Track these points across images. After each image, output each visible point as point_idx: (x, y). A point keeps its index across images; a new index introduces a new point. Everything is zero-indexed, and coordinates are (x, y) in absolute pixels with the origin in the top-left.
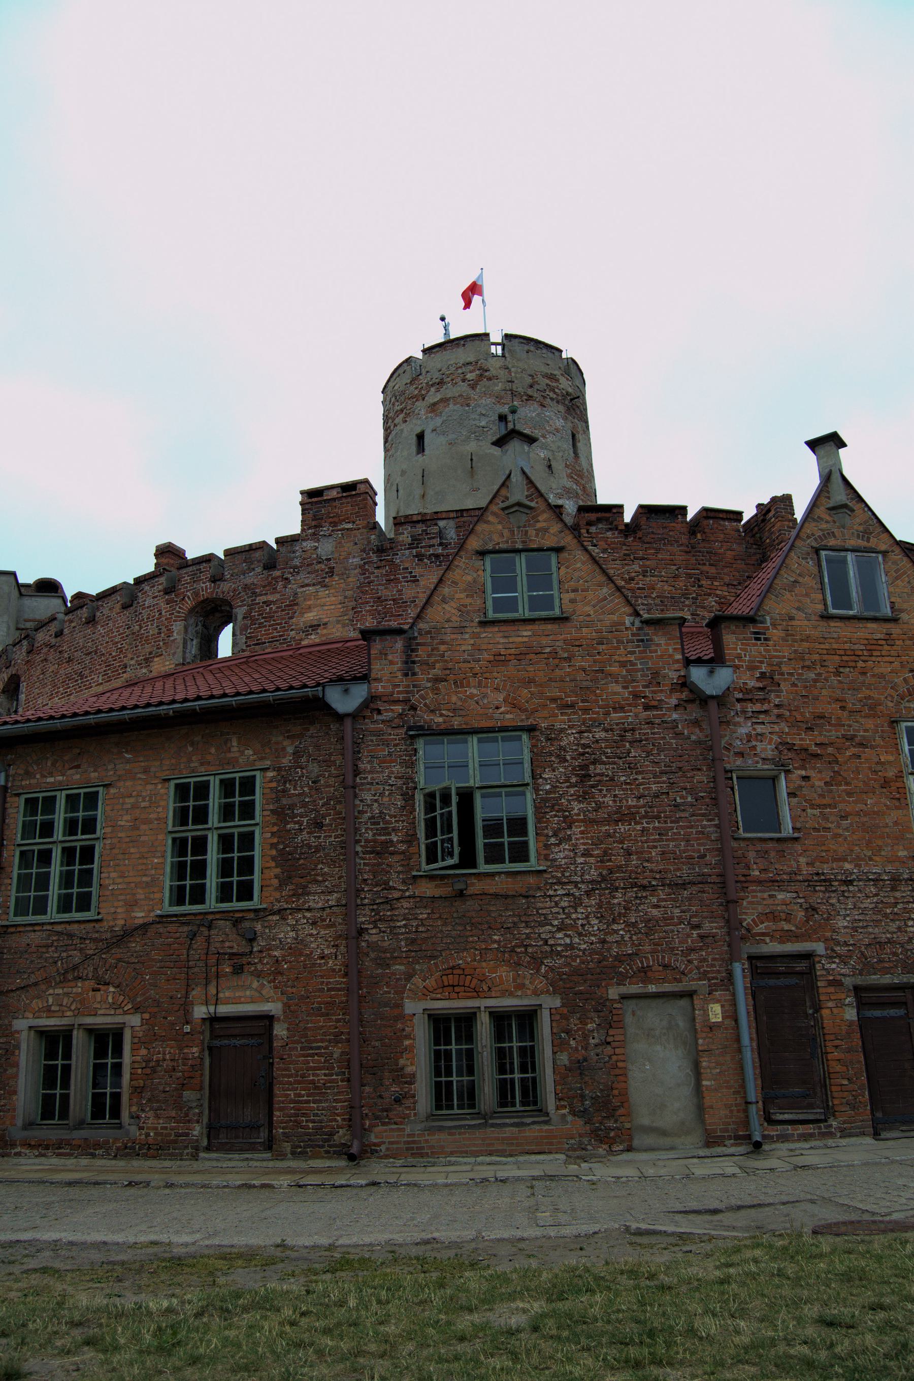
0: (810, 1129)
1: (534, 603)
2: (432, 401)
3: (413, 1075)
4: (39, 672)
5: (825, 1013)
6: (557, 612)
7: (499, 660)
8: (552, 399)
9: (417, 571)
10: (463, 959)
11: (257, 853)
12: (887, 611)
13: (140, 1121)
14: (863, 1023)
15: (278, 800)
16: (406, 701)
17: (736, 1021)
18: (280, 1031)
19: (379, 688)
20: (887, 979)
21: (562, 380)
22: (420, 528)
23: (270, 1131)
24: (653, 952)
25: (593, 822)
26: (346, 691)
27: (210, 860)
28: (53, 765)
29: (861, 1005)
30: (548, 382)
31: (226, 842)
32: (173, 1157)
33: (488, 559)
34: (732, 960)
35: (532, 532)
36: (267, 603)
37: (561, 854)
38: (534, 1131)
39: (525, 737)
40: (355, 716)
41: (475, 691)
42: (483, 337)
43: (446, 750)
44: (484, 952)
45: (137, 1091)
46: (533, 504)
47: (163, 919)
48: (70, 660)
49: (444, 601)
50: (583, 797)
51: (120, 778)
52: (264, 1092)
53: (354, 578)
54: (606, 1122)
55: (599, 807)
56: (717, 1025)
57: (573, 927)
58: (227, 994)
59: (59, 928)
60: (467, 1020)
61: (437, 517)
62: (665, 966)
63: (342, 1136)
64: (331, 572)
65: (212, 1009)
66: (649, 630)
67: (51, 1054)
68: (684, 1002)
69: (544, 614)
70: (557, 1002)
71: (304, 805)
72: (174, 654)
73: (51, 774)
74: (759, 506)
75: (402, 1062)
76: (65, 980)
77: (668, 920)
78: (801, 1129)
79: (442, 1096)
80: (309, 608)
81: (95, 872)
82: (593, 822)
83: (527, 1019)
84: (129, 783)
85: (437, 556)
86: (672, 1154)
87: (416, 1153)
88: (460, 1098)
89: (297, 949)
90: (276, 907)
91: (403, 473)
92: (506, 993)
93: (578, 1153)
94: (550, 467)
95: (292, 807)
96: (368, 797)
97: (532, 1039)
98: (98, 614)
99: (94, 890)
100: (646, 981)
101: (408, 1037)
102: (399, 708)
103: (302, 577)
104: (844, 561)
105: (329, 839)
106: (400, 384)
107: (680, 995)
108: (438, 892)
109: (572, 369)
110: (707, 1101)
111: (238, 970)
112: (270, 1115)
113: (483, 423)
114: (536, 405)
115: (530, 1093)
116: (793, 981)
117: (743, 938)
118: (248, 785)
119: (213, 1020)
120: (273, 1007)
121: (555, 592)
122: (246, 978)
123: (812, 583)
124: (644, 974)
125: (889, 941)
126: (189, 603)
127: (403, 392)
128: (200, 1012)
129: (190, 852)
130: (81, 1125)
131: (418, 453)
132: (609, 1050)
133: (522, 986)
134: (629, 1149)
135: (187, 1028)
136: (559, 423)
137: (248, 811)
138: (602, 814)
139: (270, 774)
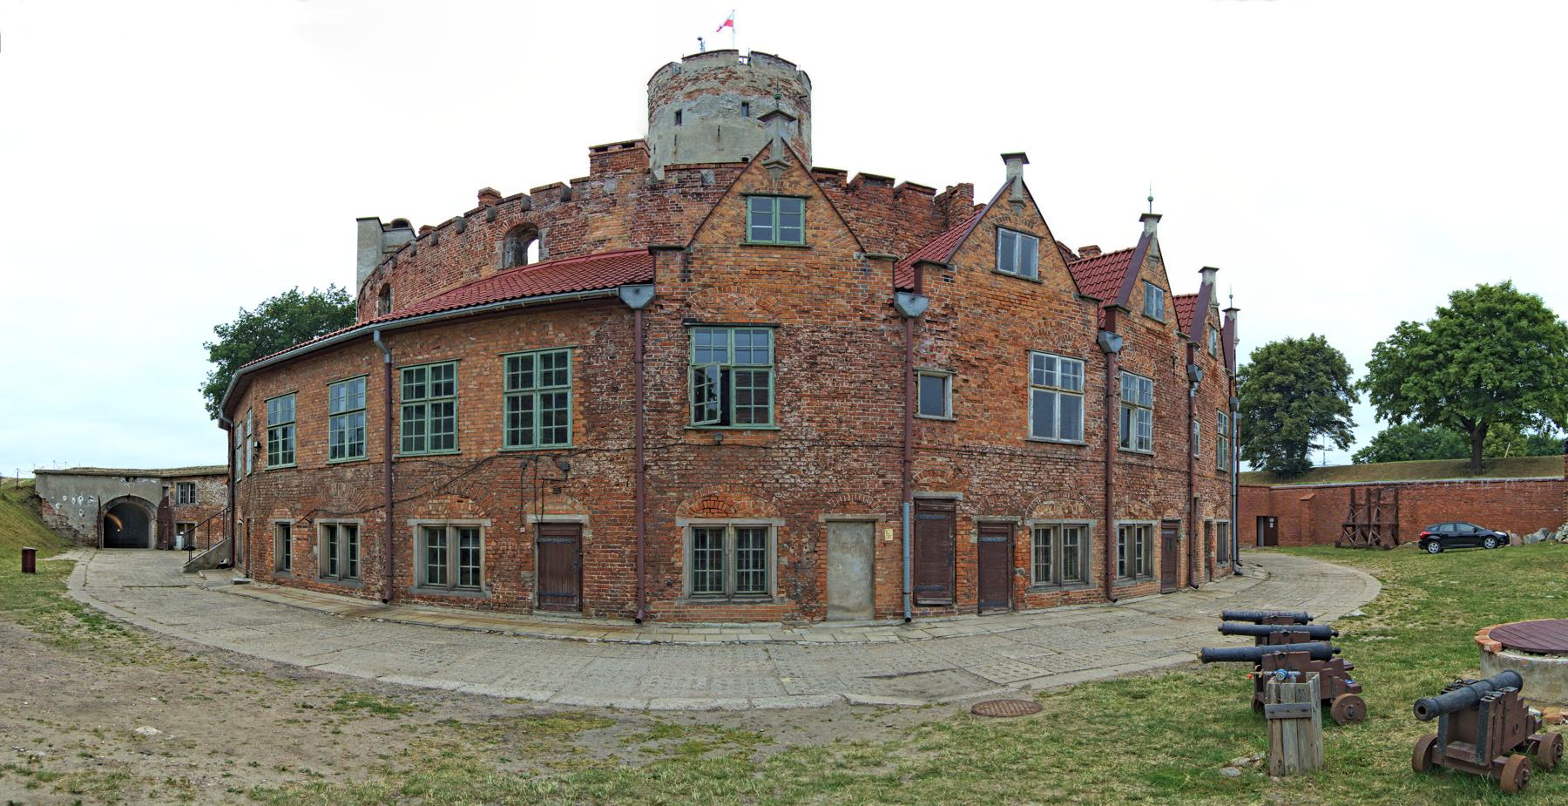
0: (940, 610)
10: (718, 490)
11: (569, 408)
13: (492, 587)
14: (981, 545)
15: (584, 370)
16: (683, 300)
18: (587, 534)
19: (662, 290)
20: (998, 518)
22: (685, 174)
25: (817, 397)
26: (637, 292)
27: (535, 411)
29: (981, 533)
31: (547, 400)
32: (515, 612)
33: (750, 200)
34: (903, 501)
36: (565, 225)
37: (792, 419)
39: (771, 332)
43: (713, 338)
44: (733, 486)
45: (490, 569)
47: (504, 454)
50: (810, 379)
53: (632, 207)
54: (810, 601)
55: (822, 386)
56: (890, 543)
60: (718, 532)
63: (631, 606)
64: (614, 203)
67: (432, 541)
68: (869, 526)
70: (783, 523)
71: (604, 374)
77: (863, 470)
78: (935, 610)
79: (699, 582)
82: (817, 397)
83: (761, 532)
86: (852, 624)
87: (681, 618)
89: (599, 478)
93: (791, 622)
95: (595, 376)
96: (652, 370)
97: (763, 545)
100: (845, 511)
102: (677, 305)
103: (592, 207)
105: (623, 400)
107: (867, 522)
108: (702, 442)
111: (557, 491)
112: (581, 589)
115: (760, 581)
116: (943, 516)
118: (562, 359)
119: (540, 524)
120: (583, 518)
122: (563, 497)
124: (844, 506)
128: (531, 519)
129: (520, 406)
130: (454, 587)
133: (758, 511)
134: (824, 620)
137: (562, 378)
138: (824, 392)
139: (578, 351)
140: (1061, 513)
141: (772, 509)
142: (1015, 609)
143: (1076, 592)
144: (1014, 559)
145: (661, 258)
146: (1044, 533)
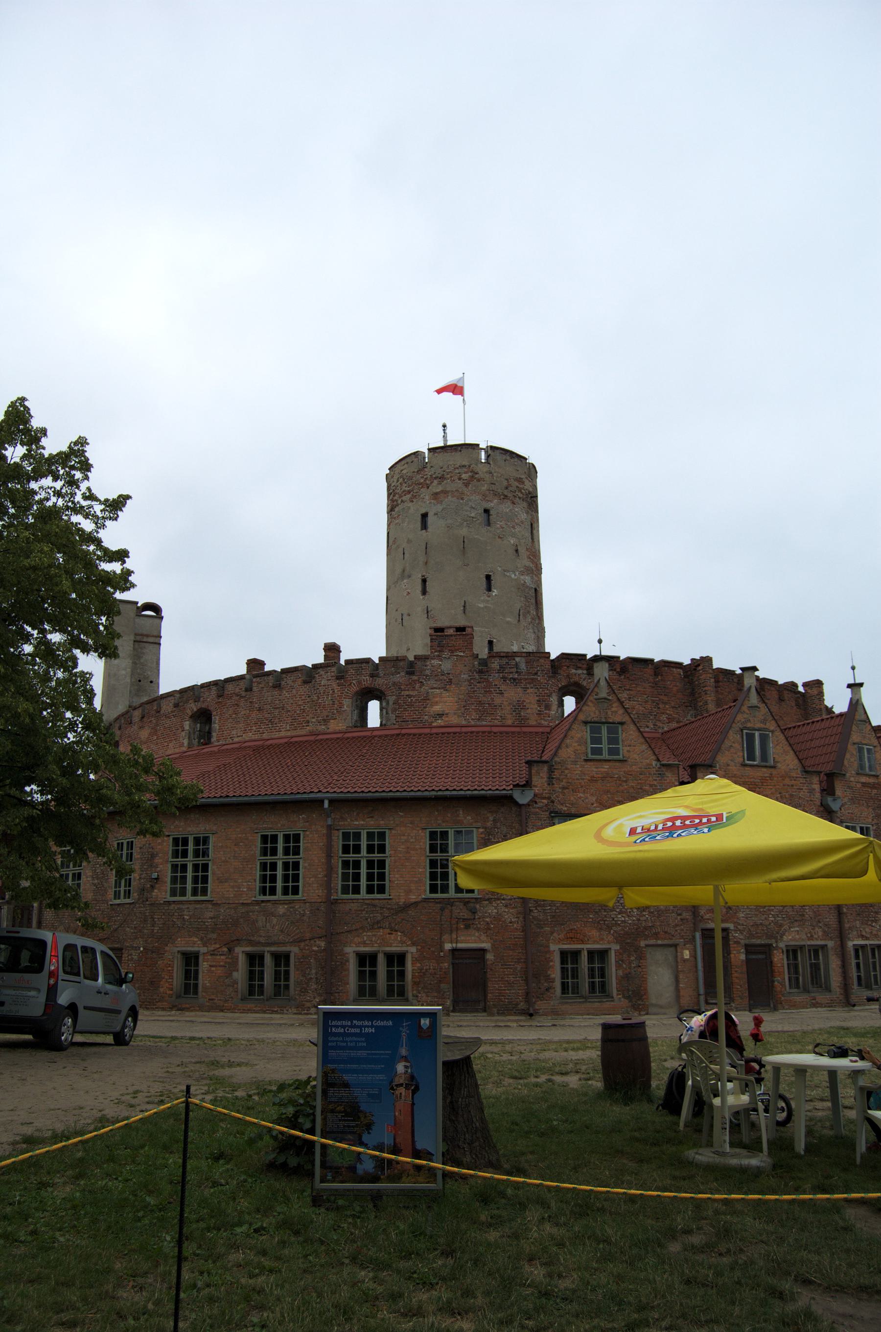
1: (612, 752)
2: (435, 491)
3: (554, 979)
4: (230, 712)
5: (732, 955)
6: (621, 757)
7: (593, 780)
8: (520, 498)
9: (503, 687)
12: (772, 763)
14: (748, 961)
16: (549, 798)
17: (696, 958)
18: (489, 956)
19: (536, 790)
20: (758, 942)
21: (527, 482)
22: (505, 661)
23: (485, 1003)
24: (660, 925)
28: (358, 814)
29: (747, 953)
30: (517, 484)
33: (588, 726)
34: (695, 931)
35: (609, 713)
36: (409, 696)
38: (607, 1005)
40: (528, 805)
41: (582, 795)
42: (475, 447)
45: (416, 984)
46: (610, 698)
47: (426, 900)
48: (260, 710)
49: (567, 747)
51: (397, 825)
52: (481, 985)
57: (625, 912)
58: (462, 938)
59: (367, 902)
60: (576, 954)
61: (514, 655)
62: (666, 932)
65: (454, 945)
66: (664, 769)
68: (672, 949)
69: (615, 757)
70: (618, 947)
72: (345, 720)
73: (356, 820)
74: (692, 660)
75: (549, 972)
76: (373, 928)
79: (564, 987)
80: (437, 703)
81: (387, 874)
83: (603, 954)
84: (403, 829)
85: (515, 679)
86: (665, 1016)
87: (555, 1013)
88: (572, 990)
90: (487, 897)
91: (409, 541)
92: (595, 942)
94: (517, 551)
98: (283, 683)
99: (387, 883)
101: (552, 961)
102: (545, 801)
103: (432, 682)
104: (754, 734)
106: (407, 471)
109: (532, 471)
110: (682, 993)
111: (467, 927)
112: (485, 996)
113: (473, 515)
114: (509, 503)
115: (603, 987)
117: (700, 921)
119: (454, 950)
121: (620, 746)
123: (737, 746)
124: (656, 936)
125: (761, 924)
126: (355, 689)
127: (411, 478)
128: (448, 946)
131: (422, 529)
132: (640, 970)
134: (647, 1014)
135: (442, 954)
136: (523, 516)
139: (481, 830)
140: (804, 937)
141: (611, 938)
142: (775, 1009)
143: (821, 997)
144: (772, 971)
145: (534, 769)
146: (793, 952)
